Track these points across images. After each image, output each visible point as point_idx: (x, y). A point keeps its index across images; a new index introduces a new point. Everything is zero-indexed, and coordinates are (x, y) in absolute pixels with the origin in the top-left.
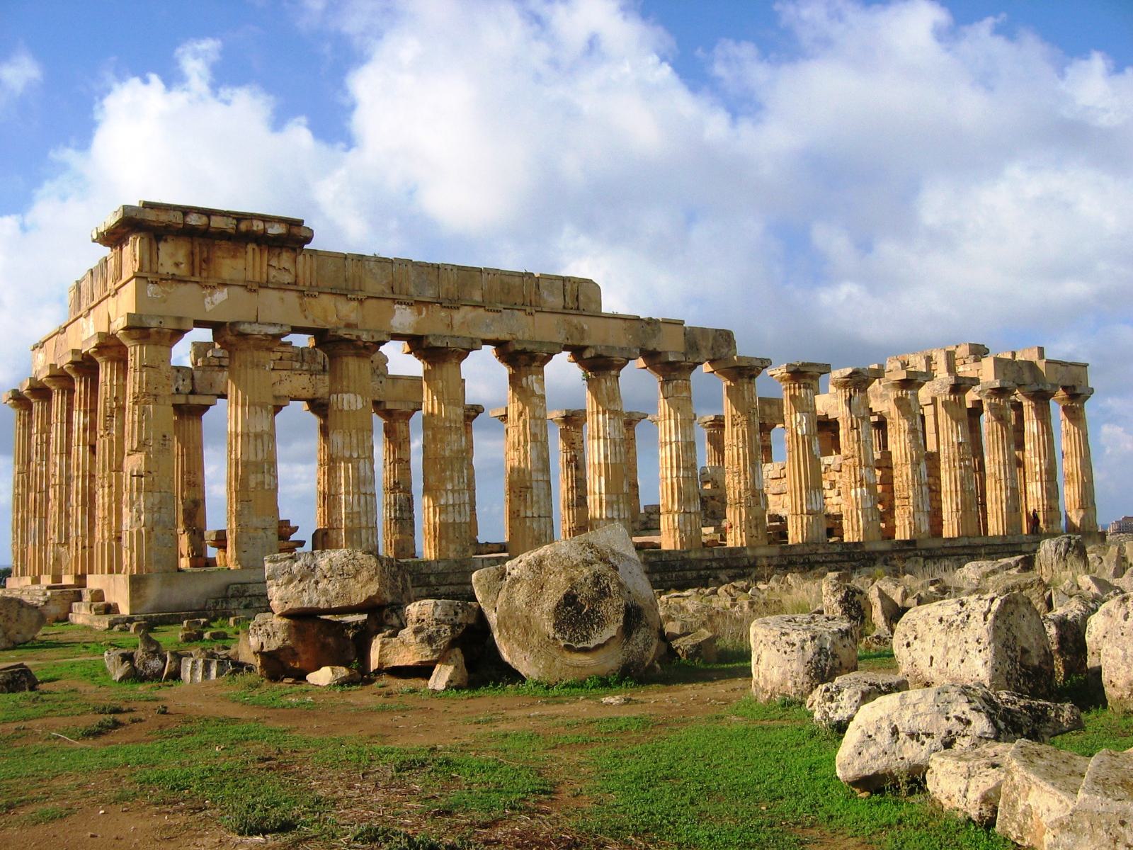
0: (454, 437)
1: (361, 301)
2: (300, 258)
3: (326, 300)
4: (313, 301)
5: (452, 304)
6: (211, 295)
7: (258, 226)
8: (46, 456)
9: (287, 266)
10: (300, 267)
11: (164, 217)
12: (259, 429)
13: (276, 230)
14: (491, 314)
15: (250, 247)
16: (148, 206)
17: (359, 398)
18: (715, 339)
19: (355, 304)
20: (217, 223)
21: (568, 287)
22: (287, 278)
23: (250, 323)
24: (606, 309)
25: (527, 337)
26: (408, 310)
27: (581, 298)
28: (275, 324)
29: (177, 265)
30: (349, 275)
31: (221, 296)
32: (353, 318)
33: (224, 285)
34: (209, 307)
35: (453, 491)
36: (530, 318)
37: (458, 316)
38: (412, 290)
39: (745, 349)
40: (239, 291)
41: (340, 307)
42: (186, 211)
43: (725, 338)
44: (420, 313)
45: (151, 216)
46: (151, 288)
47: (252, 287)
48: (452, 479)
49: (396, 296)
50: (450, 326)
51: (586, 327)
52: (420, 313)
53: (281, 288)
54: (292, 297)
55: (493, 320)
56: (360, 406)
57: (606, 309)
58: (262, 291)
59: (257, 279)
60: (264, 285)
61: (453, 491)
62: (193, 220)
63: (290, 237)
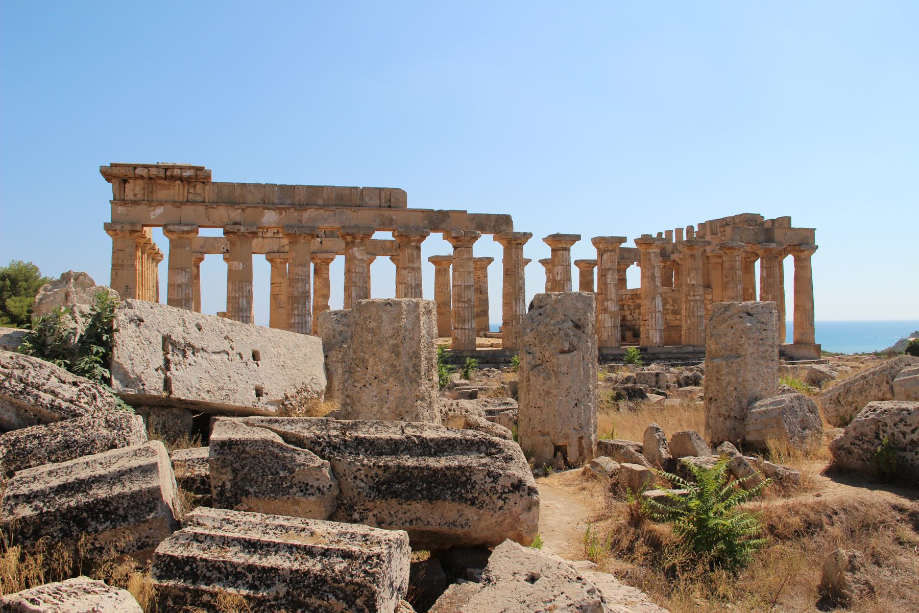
0: (300, 284)
1: (243, 210)
2: (207, 187)
4: (214, 211)
5: (302, 207)
6: (154, 210)
7: (177, 172)
9: (199, 192)
10: (206, 192)
11: (122, 171)
12: (179, 282)
13: (186, 174)
14: (328, 213)
16: (113, 165)
17: (241, 264)
18: (497, 220)
19: (240, 211)
20: (154, 172)
21: (383, 194)
22: (199, 199)
23: (174, 225)
24: (410, 205)
26: (273, 213)
27: (392, 200)
28: (186, 225)
29: (135, 195)
30: (235, 196)
31: (159, 210)
32: (238, 219)
33: (162, 205)
34: (152, 217)
35: (298, 315)
36: (355, 214)
38: (276, 201)
39: (518, 227)
41: (230, 213)
42: (135, 167)
44: (281, 214)
45: (115, 171)
47: (178, 204)
48: (298, 309)
49: (266, 204)
50: (300, 221)
52: (281, 214)
53: (194, 202)
54: (201, 209)
55: (329, 216)
56: (241, 268)
57: (410, 205)
58: (184, 207)
60: (182, 203)
61: (298, 315)
62: (139, 171)
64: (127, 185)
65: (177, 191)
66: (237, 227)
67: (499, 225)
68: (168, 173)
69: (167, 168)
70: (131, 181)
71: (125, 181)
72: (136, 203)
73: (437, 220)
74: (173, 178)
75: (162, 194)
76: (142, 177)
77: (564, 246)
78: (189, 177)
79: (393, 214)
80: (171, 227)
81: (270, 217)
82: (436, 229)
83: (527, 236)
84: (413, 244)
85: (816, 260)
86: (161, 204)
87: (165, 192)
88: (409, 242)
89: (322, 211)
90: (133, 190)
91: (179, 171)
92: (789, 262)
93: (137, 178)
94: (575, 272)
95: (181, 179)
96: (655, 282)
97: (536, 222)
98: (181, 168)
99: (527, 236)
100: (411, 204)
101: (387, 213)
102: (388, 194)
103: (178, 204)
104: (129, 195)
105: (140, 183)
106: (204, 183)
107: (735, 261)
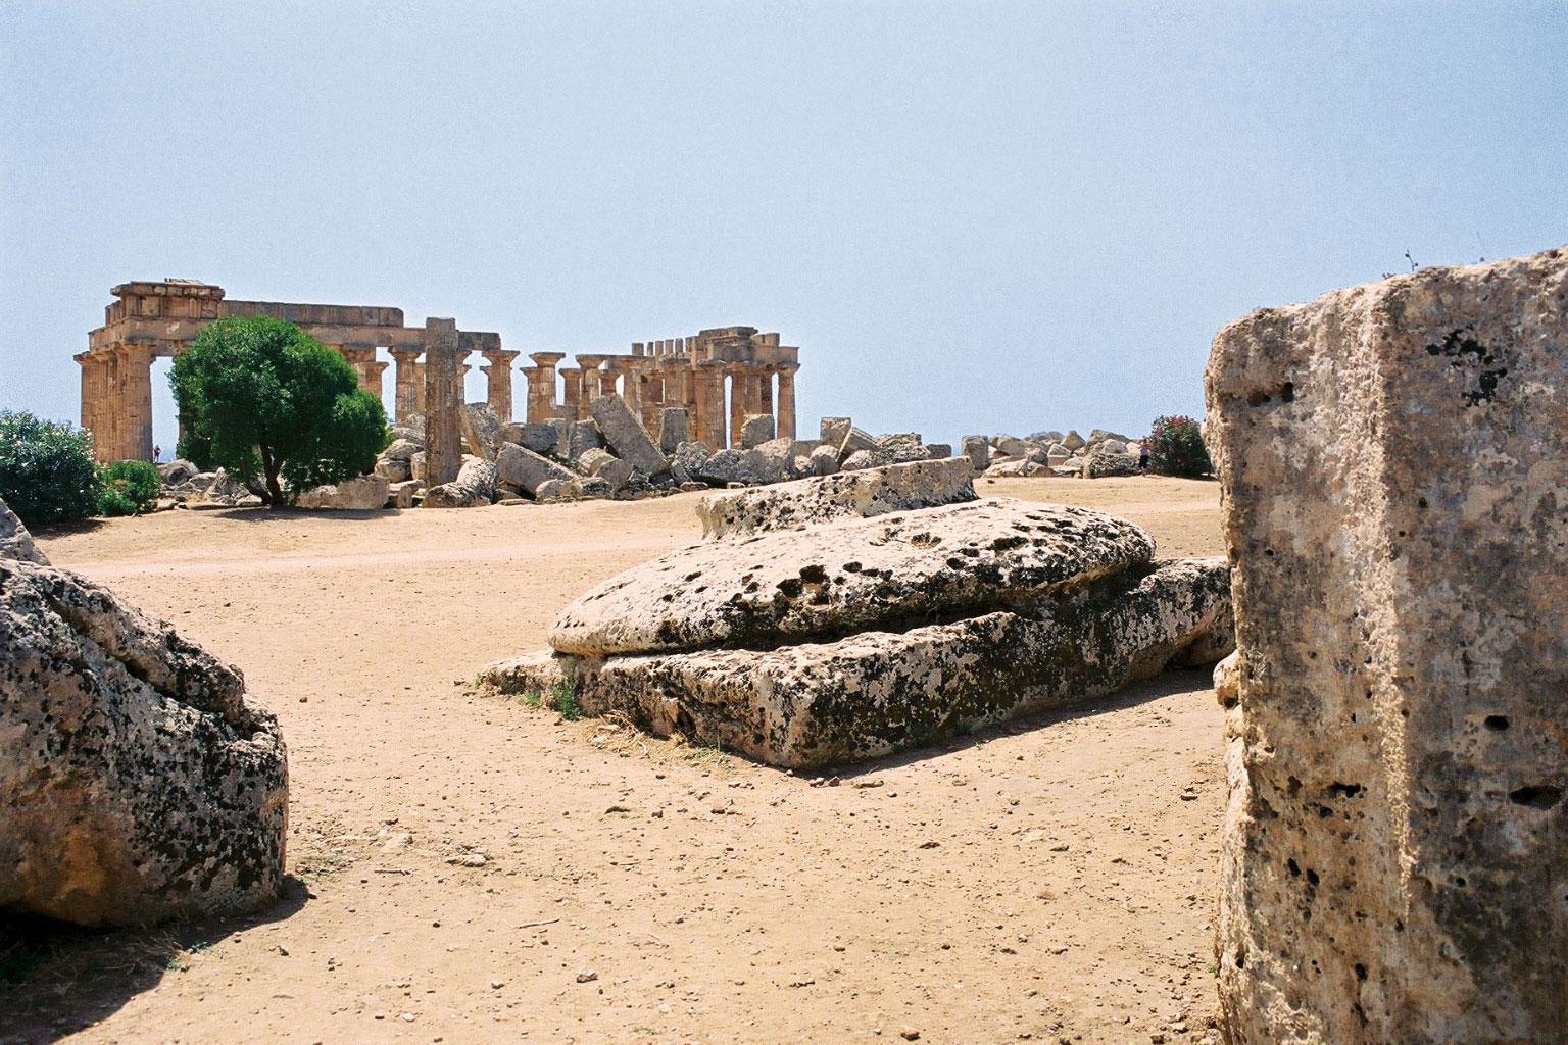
9: (210, 308)
11: (143, 290)
20: (172, 290)
29: (152, 311)
31: (175, 326)
40: (184, 322)
42: (154, 285)
43: (495, 336)
47: (192, 320)
62: (157, 290)
63: (215, 294)
65: (191, 308)
67: (489, 342)
69: (184, 287)
71: (141, 298)
72: (153, 319)
74: (189, 296)
76: (158, 295)
79: (392, 332)
83: (515, 354)
85: (798, 378)
86: (176, 319)
87: (179, 309)
90: (149, 306)
92: (775, 378)
93: (154, 295)
94: (560, 381)
95: (197, 297)
97: (522, 343)
98: (197, 287)
99: (515, 354)
101: (385, 331)
103: (192, 320)
104: (146, 311)
105: (156, 299)
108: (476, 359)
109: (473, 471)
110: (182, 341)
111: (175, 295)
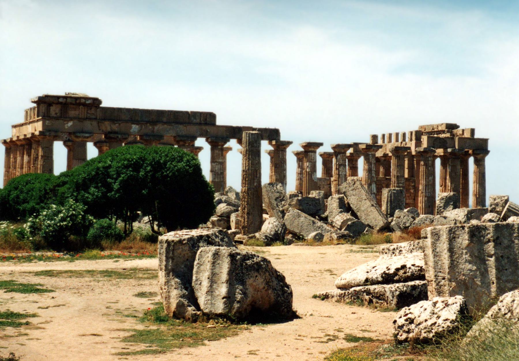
1: (120, 124)
3: (107, 123)
6: (67, 123)
7: (83, 101)
8: (15, 168)
11: (52, 100)
13: (88, 102)
15: (81, 107)
19: (117, 125)
20: (69, 100)
22: (93, 117)
23: (79, 133)
25: (184, 133)
31: (70, 124)
33: (72, 120)
34: (66, 127)
37: (156, 128)
40: (76, 121)
45: (47, 100)
46: (47, 122)
47: (81, 120)
50: (153, 131)
51: (209, 130)
54: (95, 123)
59: (83, 117)
62: (61, 100)
63: (96, 102)
64: (51, 107)
65: (81, 112)
66: (116, 135)
67: (272, 134)
68: (78, 102)
70: (54, 105)
72: (57, 118)
73: (235, 132)
74: (80, 104)
75: (72, 113)
77: (313, 149)
78: (89, 104)
79: (209, 129)
80: (78, 135)
81: (135, 128)
82: (233, 137)
83: (289, 143)
84: (219, 147)
85: (488, 160)
86: (71, 119)
88: (218, 145)
89: (166, 126)
90: (54, 110)
91: (84, 101)
95: (84, 105)
96: (371, 174)
97: (295, 136)
99: (289, 143)
100: (220, 122)
101: (204, 128)
102: (205, 115)
103: (81, 120)
106: (96, 107)
107: (429, 161)
108: (265, 146)
109: (271, 226)
110: (74, 133)
111: (71, 104)
